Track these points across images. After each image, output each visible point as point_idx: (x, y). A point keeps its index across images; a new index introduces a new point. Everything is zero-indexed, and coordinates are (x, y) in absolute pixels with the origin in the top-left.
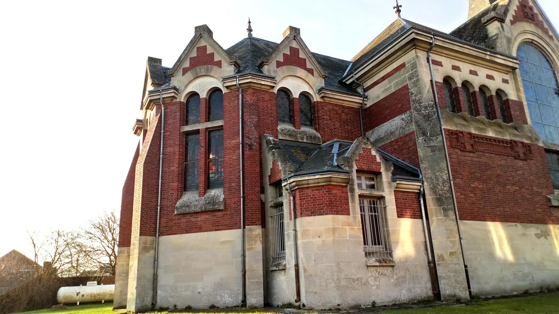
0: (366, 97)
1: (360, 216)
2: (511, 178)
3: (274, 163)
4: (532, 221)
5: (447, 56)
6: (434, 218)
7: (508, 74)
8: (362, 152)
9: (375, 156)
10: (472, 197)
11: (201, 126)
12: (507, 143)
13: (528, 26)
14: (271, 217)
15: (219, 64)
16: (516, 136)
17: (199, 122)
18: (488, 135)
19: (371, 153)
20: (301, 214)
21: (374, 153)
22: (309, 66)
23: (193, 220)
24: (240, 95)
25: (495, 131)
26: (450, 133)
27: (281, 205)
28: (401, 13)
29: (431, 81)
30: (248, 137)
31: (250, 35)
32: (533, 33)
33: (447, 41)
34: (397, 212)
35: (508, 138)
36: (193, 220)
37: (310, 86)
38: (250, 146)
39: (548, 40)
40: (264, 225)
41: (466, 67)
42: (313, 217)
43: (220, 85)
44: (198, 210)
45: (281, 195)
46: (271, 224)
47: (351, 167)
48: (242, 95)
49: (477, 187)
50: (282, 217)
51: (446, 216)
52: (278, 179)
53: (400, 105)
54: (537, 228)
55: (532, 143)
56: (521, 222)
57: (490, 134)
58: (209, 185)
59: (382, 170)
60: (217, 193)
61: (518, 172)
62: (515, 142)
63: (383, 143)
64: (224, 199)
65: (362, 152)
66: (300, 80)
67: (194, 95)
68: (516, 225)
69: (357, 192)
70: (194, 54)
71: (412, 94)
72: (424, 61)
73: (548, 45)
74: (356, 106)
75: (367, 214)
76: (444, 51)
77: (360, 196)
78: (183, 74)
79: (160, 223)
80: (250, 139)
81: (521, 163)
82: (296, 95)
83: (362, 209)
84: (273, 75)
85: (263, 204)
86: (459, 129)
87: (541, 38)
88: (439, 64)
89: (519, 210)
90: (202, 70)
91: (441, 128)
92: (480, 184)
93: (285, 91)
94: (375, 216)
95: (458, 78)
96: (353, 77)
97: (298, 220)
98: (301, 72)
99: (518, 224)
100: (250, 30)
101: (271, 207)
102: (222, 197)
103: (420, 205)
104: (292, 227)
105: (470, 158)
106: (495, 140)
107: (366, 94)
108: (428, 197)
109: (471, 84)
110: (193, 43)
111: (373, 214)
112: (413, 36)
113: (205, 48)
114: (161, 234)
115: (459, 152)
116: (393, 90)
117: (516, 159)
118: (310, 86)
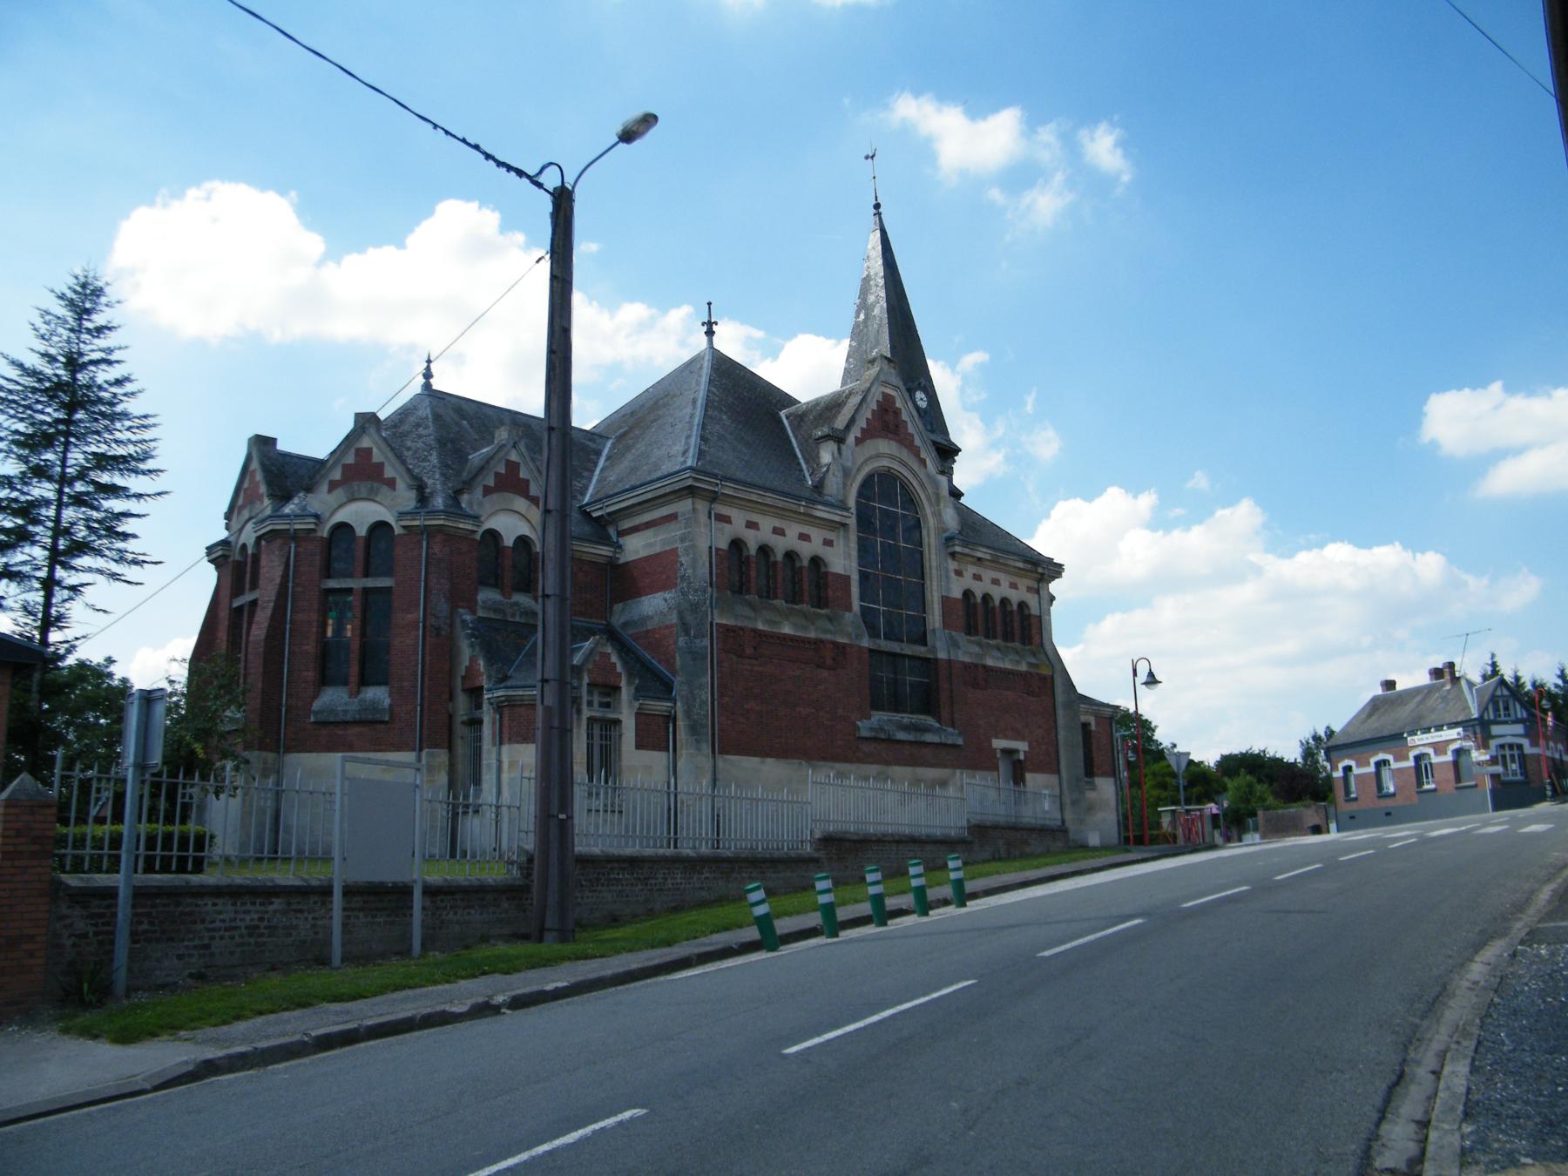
0: (620, 547)
1: (585, 746)
2: (805, 696)
3: (473, 660)
5: (741, 508)
6: (684, 752)
8: (597, 658)
9: (615, 664)
11: (357, 583)
12: (809, 643)
13: (885, 446)
14: (462, 738)
15: (391, 483)
16: (826, 631)
17: (351, 576)
18: (783, 632)
19: (609, 659)
20: (510, 739)
21: (614, 659)
22: (534, 490)
23: (340, 732)
24: (424, 543)
25: (795, 626)
26: (727, 631)
27: (480, 722)
28: (714, 338)
29: (711, 548)
30: (434, 615)
31: (427, 386)
32: (891, 457)
35: (812, 635)
36: (340, 732)
37: (532, 526)
38: (438, 629)
39: (916, 466)
40: (450, 748)
41: (767, 523)
42: (524, 745)
43: (391, 520)
44: (349, 717)
45: (479, 706)
46: (461, 749)
47: (580, 679)
48: (428, 543)
50: (479, 739)
51: (699, 749)
52: (478, 684)
53: (664, 577)
57: (787, 629)
58: (364, 681)
59: (623, 684)
60: (378, 695)
62: (822, 641)
63: (636, 631)
64: (390, 705)
65: (597, 658)
66: (517, 516)
67: (344, 527)
68: (800, 763)
69: (586, 713)
70: (350, 459)
71: (682, 565)
72: (703, 518)
73: (915, 475)
74: (602, 560)
75: (597, 742)
76: (736, 501)
77: (589, 719)
78: (330, 491)
79: (285, 734)
80: (437, 618)
81: (825, 674)
82: (509, 541)
83: (590, 736)
84: (476, 510)
85: (451, 717)
86: (739, 624)
87: (905, 464)
88: (726, 519)
90: (363, 488)
91: (711, 624)
93: (493, 535)
95: (752, 540)
96: (601, 508)
97: (505, 748)
98: (520, 504)
100: (428, 375)
101: (463, 723)
102: (387, 701)
103: (668, 732)
104: (494, 756)
105: (749, 668)
106: (791, 640)
107: (621, 541)
108: (681, 723)
109: (772, 550)
110: (349, 440)
111: (604, 743)
112: (690, 482)
113: (369, 451)
114: (288, 750)
116: (658, 549)
118: (532, 526)
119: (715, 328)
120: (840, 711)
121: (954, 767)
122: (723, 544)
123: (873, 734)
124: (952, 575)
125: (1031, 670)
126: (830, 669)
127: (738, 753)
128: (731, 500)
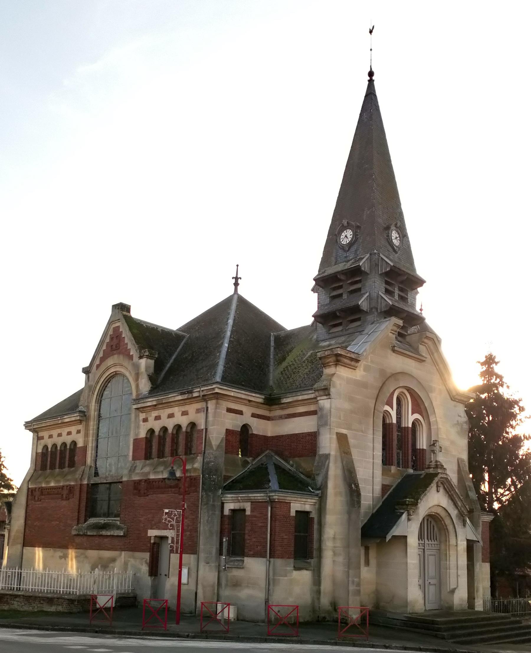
5: (46, 430)
7: (81, 424)
33: (38, 423)
54: (62, 552)
57: (52, 484)
68: (50, 550)
81: (64, 503)
119: (239, 281)
124: (141, 423)
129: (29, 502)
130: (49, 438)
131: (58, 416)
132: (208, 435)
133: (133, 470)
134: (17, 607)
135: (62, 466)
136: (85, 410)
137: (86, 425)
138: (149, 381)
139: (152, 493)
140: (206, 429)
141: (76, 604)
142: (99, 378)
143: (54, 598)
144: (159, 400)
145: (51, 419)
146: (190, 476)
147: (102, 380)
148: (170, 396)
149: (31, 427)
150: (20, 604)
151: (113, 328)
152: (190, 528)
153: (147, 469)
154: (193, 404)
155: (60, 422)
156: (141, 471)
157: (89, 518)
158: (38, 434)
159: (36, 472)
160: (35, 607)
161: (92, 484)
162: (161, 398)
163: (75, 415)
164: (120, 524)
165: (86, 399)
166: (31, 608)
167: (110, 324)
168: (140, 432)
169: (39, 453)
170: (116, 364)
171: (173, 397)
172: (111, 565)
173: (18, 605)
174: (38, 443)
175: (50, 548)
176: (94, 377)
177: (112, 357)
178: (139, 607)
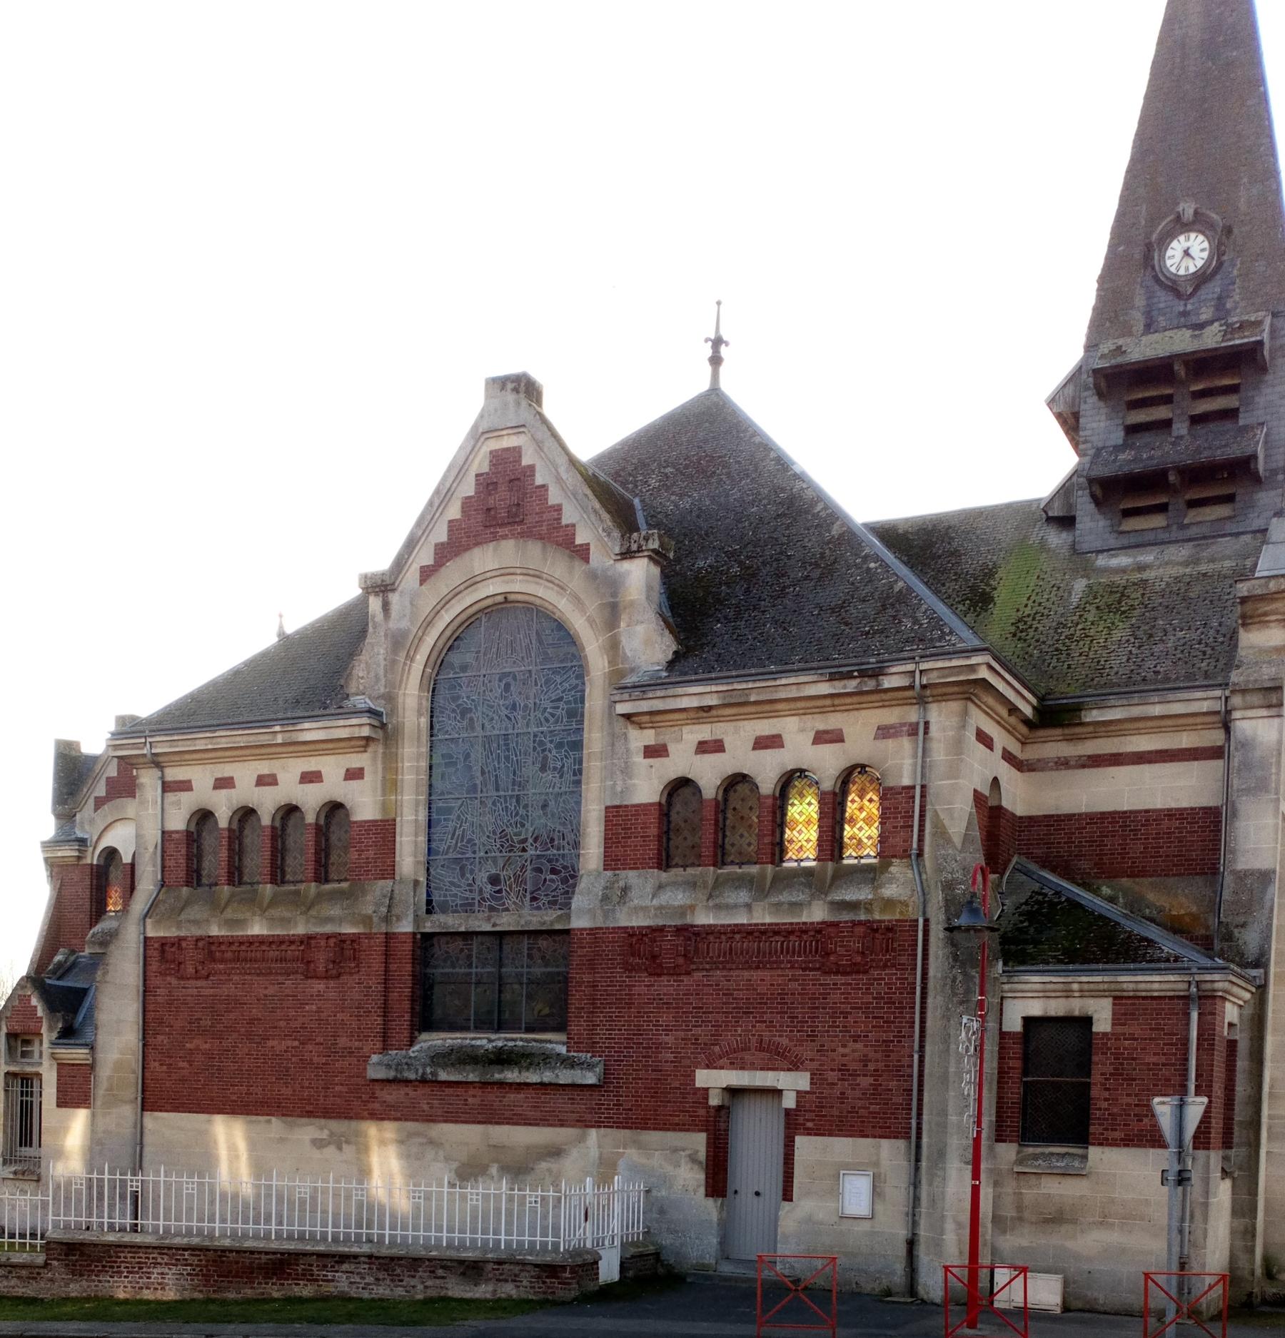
4: (311, 1112)
5: (201, 762)
7: (365, 751)
10: (183, 1068)
18: (249, 933)
25: (272, 920)
33: (176, 738)
34: (58, 1098)
35: (300, 929)
41: (245, 773)
49: (197, 1049)
54: (321, 1129)
55: (367, 931)
56: (283, 1115)
57: (257, 928)
61: (307, 1007)
68: (269, 1122)
81: (318, 986)
88: (185, 786)
89: (284, 1090)
92: (206, 1042)
94: (27, 1101)
99: (273, 1119)
115: (174, 981)
117: (307, 977)
120: (343, 1041)
121: (584, 1123)
122: (178, 822)
123: (391, 1074)
124: (639, 759)
125: (846, 917)
126: (327, 977)
127: (176, 1109)
128: (181, 758)
129: (155, 981)
130: (215, 787)
131: (276, 720)
132: (932, 805)
133: (616, 899)
134: (346, 1289)
135: (277, 874)
136: (382, 710)
137: (384, 753)
138: (667, 632)
139: (707, 967)
140: (923, 787)
141: (567, 1278)
142: (436, 613)
143: (488, 1262)
144: (735, 692)
145: (238, 729)
146: (869, 921)
147: (447, 617)
148: (784, 681)
149: (142, 749)
150: (358, 1280)
151: (491, 452)
152: (871, 1067)
153: (678, 898)
154: (863, 713)
155: (280, 741)
156: (655, 902)
157: (420, 1033)
158: (162, 771)
159: (164, 889)
160: (419, 1287)
161: (423, 934)
162: (744, 686)
163: (354, 721)
164: (568, 1051)
165: (381, 672)
166: (400, 1292)
167: (477, 441)
168: (634, 785)
169: (177, 832)
170: (512, 570)
171: (794, 687)
172: (544, 1165)
173: (351, 1283)
174: (165, 801)
175: (268, 1115)
176: (411, 604)
177: (492, 545)
178: (689, 1280)
